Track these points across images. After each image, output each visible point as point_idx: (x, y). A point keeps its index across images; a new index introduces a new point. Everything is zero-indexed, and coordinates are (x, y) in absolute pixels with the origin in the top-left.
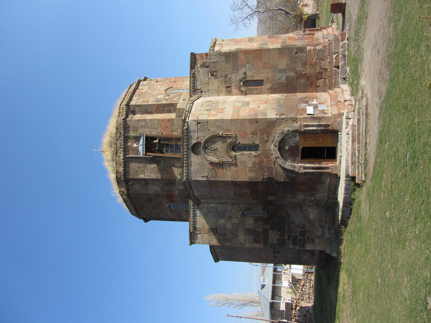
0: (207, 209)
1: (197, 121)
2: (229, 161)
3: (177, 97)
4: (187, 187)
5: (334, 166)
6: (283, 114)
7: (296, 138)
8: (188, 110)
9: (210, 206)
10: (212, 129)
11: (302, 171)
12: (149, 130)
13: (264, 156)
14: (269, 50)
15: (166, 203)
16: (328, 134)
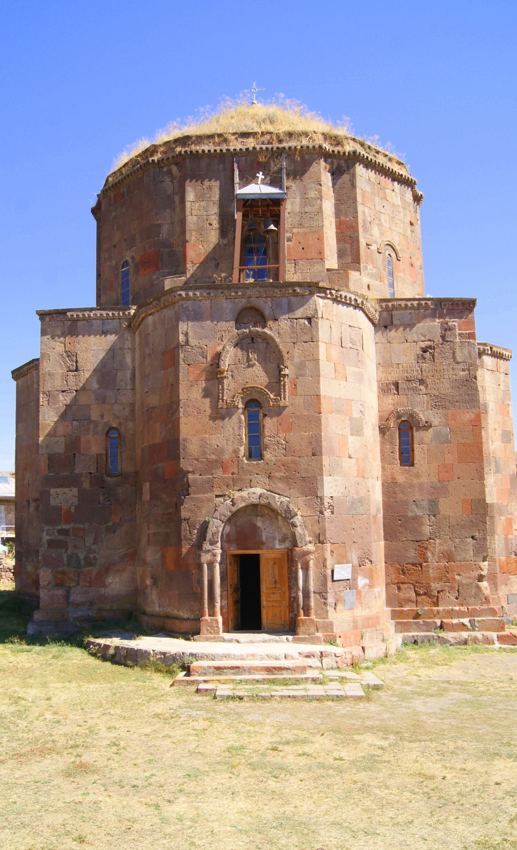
0: (121, 348)
1: (314, 317)
2: (223, 393)
3: (374, 271)
4: (162, 300)
5: (218, 627)
6: (332, 513)
7: (279, 540)
8: (341, 295)
9: (126, 354)
10: (298, 351)
11: (205, 558)
12: (297, 209)
14: (482, 478)
15: (133, 254)
16: (289, 612)
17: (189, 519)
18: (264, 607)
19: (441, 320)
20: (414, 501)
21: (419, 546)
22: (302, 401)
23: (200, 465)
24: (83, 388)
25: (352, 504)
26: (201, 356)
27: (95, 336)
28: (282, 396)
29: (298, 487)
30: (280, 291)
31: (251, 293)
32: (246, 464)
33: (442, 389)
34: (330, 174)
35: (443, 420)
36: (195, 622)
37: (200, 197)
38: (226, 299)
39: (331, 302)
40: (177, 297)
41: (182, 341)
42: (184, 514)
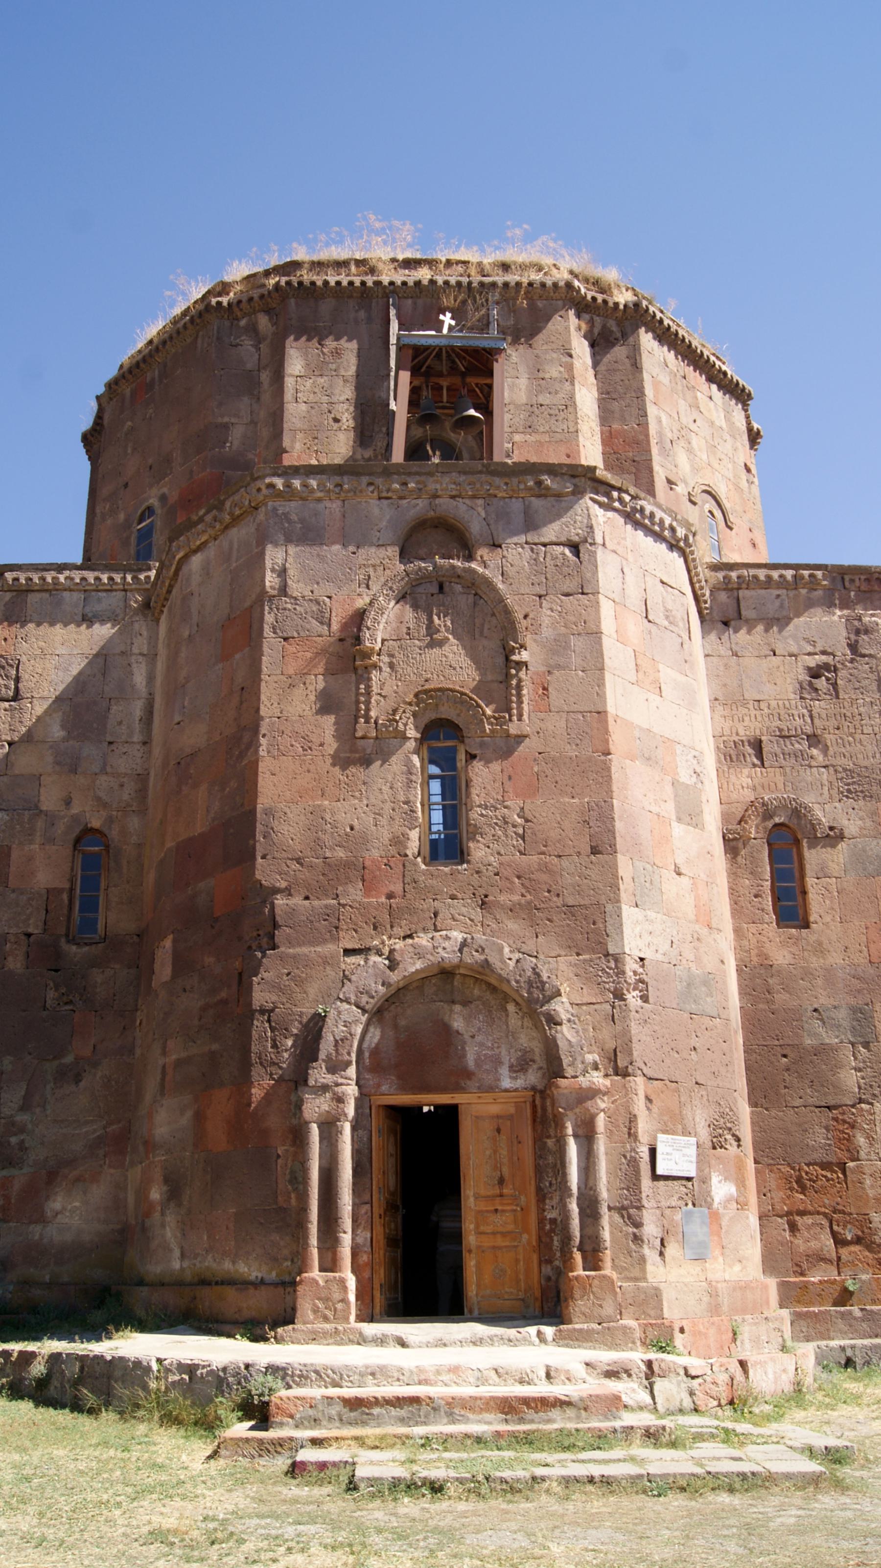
2: (368, 703)
4: (228, 504)
5: (345, 1301)
6: (645, 999)
7: (511, 1067)
8: (642, 510)
9: (134, 665)
10: (549, 612)
13: (398, 888)
15: (165, 490)
16: (540, 1263)
17: (272, 1010)
18: (470, 1251)
19: (846, 612)
20: (815, 1010)
21: (836, 1119)
22: (563, 724)
23: (304, 874)
24: (29, 737)
25: (689, 985)
26: (317, 619)
27: (65, 626)
28: (515, 711)
29: (557, 929)
30: (506, 484)
31: (438, 487)
32: (424, 873)
33: (860, 756)
34: (586, 343)
35: (869, 823)
36: (280, 1290)
37: (316, 369)
38: (380, 498)
39: (622, 520)
40: (265, 491)
41: (272, 587)
42: (260, 997)
